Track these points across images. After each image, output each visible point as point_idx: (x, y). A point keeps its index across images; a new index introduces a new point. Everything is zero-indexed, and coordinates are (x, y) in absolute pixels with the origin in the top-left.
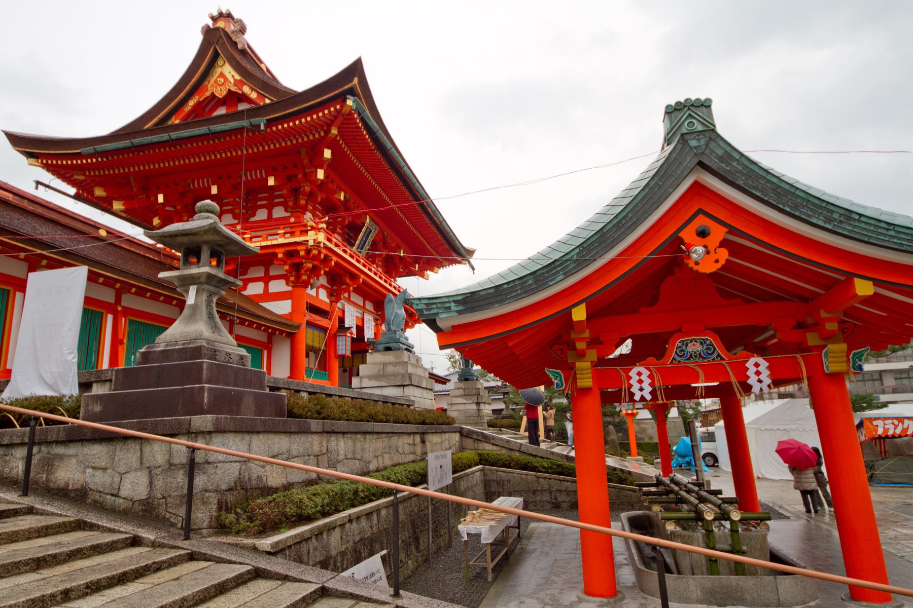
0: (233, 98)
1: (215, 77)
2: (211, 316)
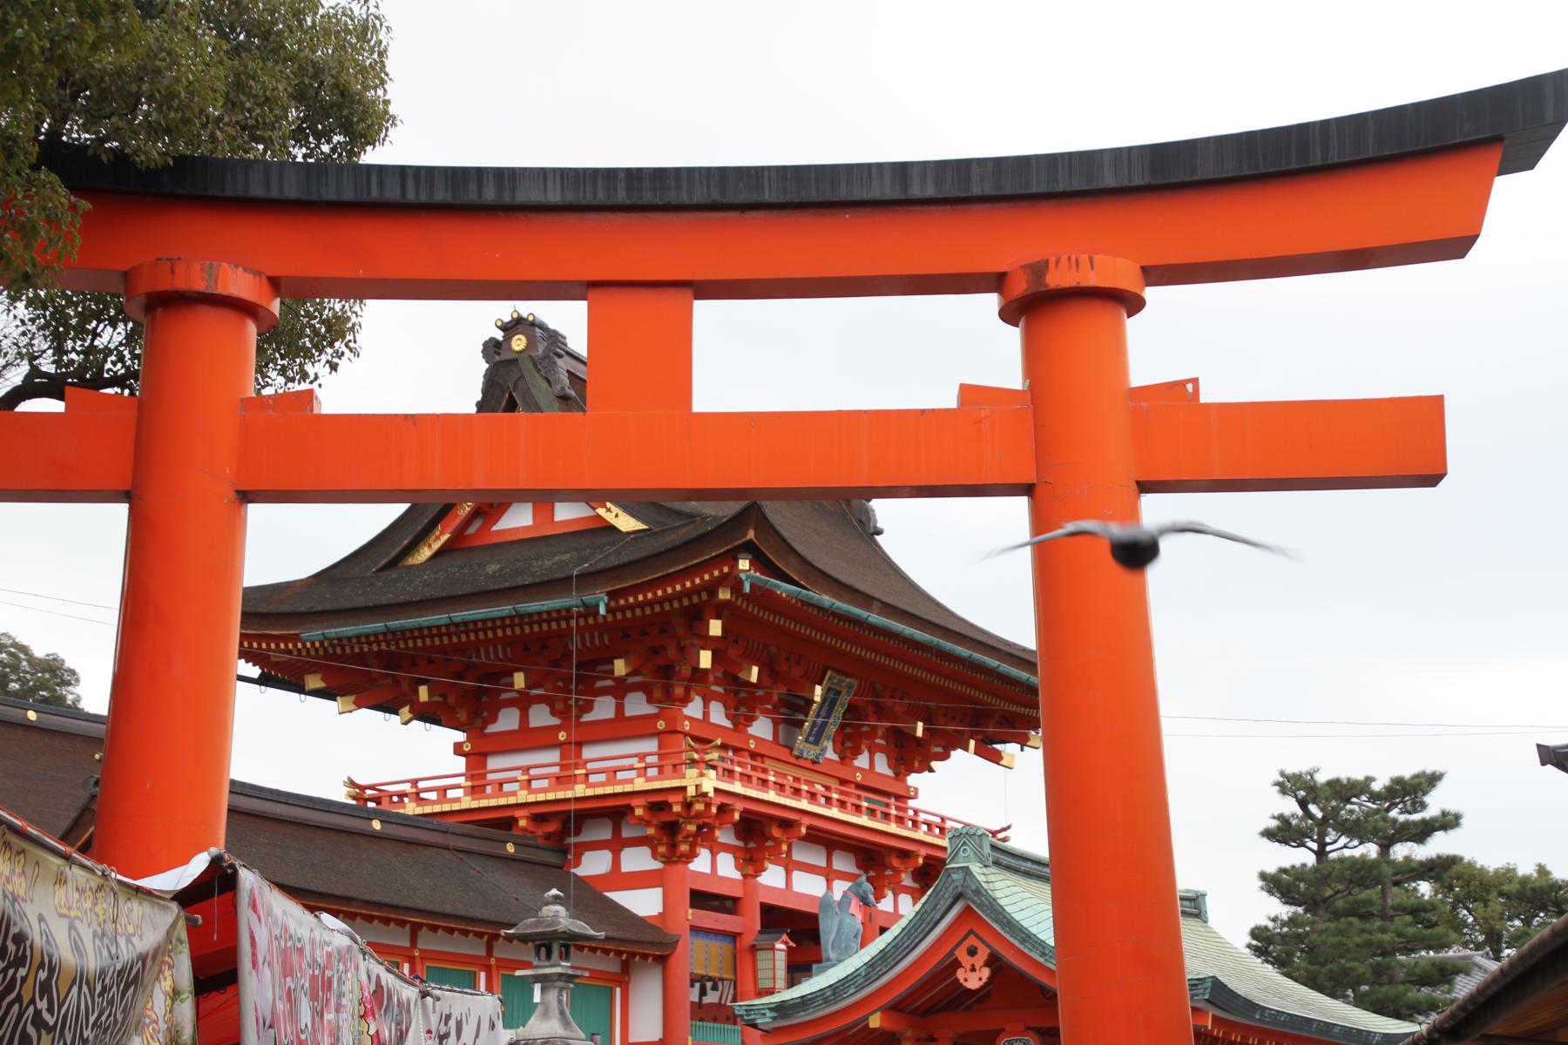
2: (562, 1013)
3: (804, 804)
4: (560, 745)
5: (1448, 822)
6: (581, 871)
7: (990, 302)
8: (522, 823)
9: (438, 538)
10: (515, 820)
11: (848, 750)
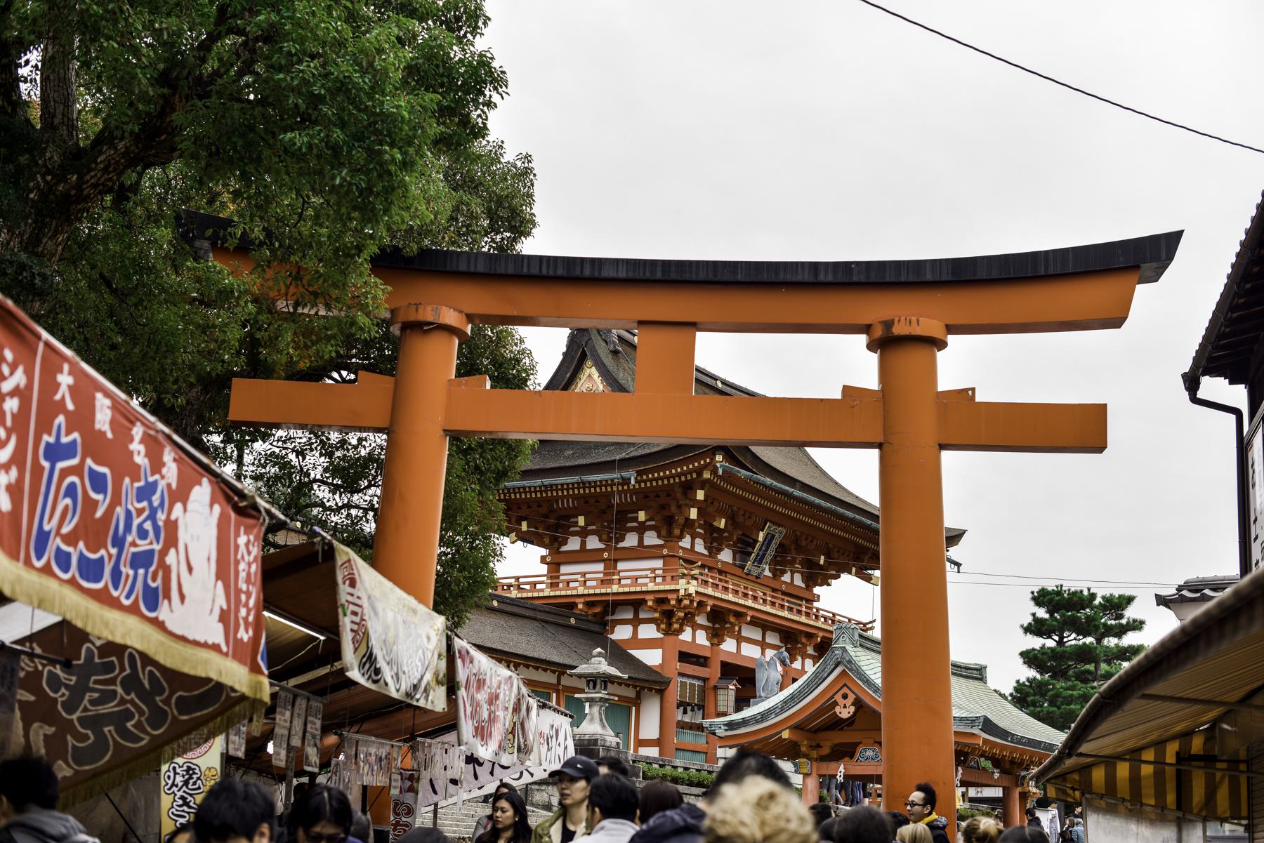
3: (750, 603)
4: (604, 560)
5: (1137, 625)
6: (613, 637)
7: (862, 339)
8: (580, 606)
10: (576, 604)
11: (777, 574)
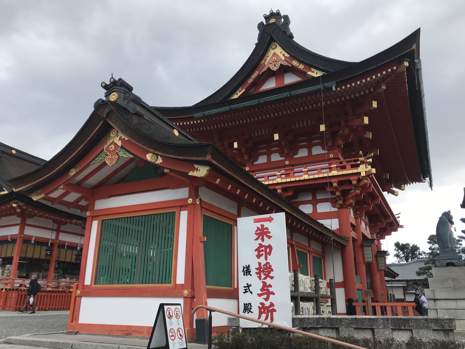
0: (284, 70)
1: (270, 57)
8: (279, 191)
9: (240, 91)
